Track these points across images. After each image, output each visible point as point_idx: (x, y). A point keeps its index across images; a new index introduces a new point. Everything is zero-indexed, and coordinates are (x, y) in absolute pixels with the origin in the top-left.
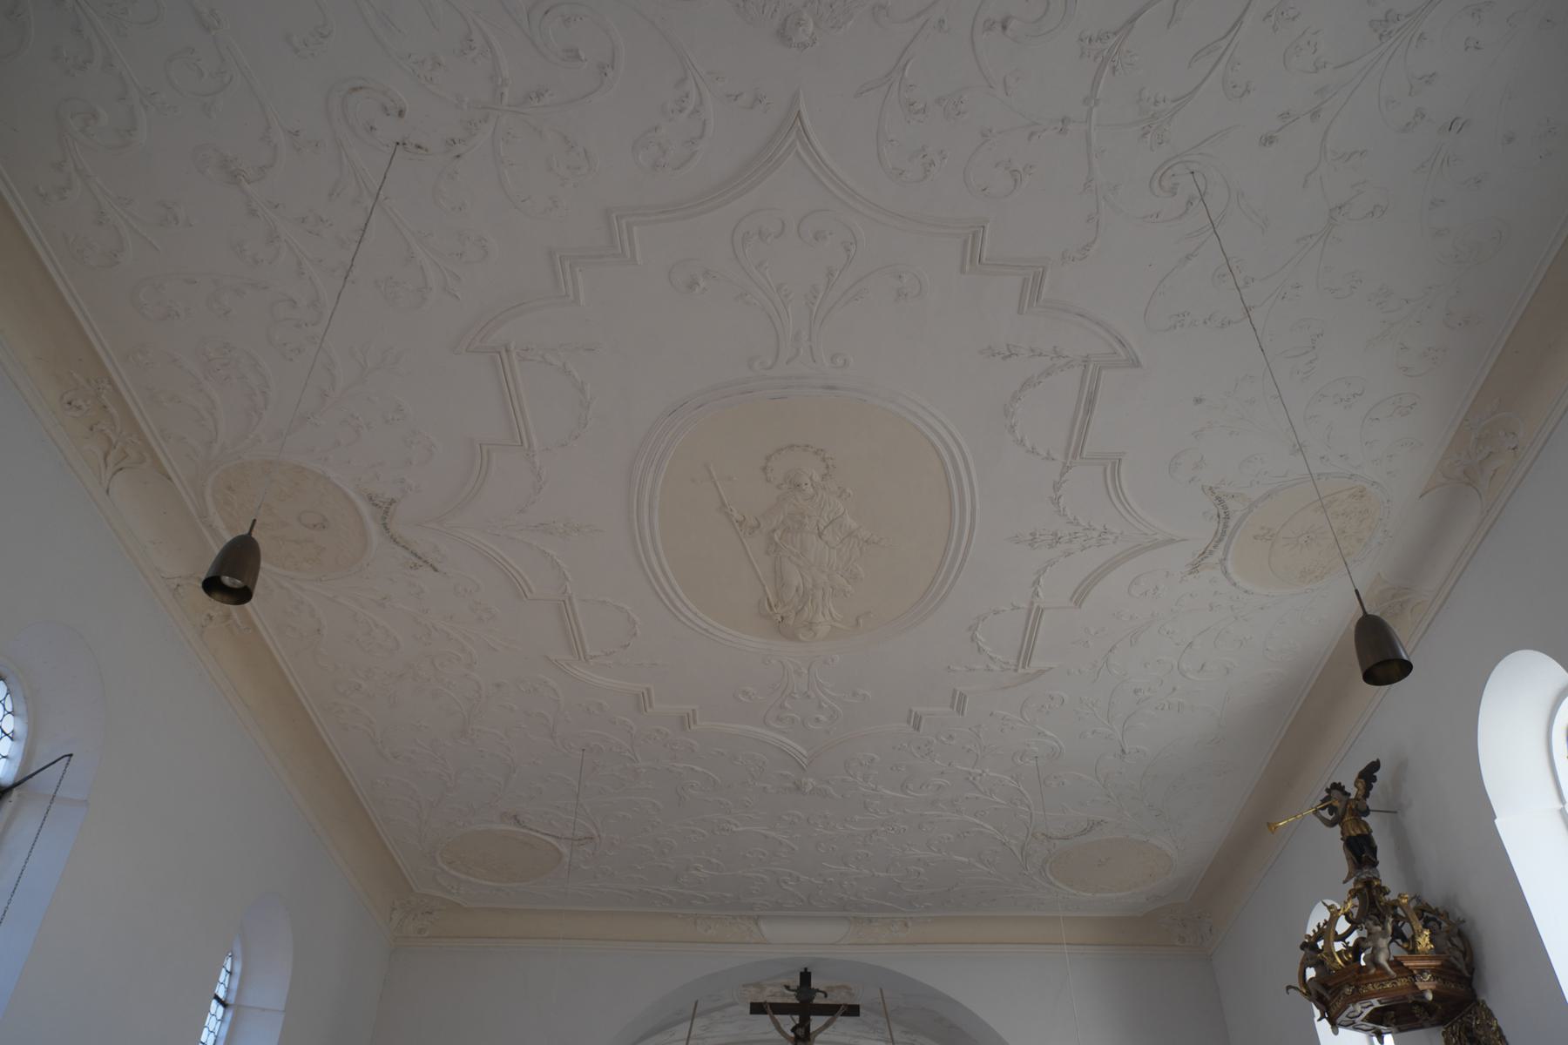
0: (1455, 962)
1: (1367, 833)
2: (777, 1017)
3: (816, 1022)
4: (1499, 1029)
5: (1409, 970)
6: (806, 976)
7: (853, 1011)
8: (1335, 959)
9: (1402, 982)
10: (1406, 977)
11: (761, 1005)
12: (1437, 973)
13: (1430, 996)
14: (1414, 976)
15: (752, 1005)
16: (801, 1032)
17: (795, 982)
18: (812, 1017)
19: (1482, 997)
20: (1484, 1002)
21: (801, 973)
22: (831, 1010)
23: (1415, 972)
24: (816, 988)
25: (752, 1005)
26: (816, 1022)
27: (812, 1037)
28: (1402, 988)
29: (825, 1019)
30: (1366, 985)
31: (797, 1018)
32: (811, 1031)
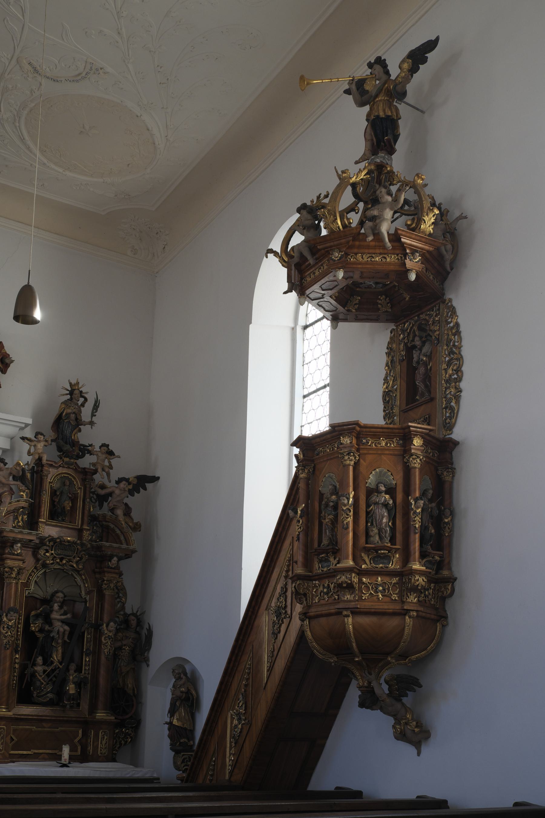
0: (445, 253)
1: (395, 118)
4: (457, 325)
5: (403, 247)
8: (336, 219)
9: (391, 259)
10: (398, 255)
12: (427, 258)
13: (413, 277)
14: (405, 255)
19: (449, 295)
20: (450, 300)
23: (408, 251)
28: (390, 264)
30: (356, 254)
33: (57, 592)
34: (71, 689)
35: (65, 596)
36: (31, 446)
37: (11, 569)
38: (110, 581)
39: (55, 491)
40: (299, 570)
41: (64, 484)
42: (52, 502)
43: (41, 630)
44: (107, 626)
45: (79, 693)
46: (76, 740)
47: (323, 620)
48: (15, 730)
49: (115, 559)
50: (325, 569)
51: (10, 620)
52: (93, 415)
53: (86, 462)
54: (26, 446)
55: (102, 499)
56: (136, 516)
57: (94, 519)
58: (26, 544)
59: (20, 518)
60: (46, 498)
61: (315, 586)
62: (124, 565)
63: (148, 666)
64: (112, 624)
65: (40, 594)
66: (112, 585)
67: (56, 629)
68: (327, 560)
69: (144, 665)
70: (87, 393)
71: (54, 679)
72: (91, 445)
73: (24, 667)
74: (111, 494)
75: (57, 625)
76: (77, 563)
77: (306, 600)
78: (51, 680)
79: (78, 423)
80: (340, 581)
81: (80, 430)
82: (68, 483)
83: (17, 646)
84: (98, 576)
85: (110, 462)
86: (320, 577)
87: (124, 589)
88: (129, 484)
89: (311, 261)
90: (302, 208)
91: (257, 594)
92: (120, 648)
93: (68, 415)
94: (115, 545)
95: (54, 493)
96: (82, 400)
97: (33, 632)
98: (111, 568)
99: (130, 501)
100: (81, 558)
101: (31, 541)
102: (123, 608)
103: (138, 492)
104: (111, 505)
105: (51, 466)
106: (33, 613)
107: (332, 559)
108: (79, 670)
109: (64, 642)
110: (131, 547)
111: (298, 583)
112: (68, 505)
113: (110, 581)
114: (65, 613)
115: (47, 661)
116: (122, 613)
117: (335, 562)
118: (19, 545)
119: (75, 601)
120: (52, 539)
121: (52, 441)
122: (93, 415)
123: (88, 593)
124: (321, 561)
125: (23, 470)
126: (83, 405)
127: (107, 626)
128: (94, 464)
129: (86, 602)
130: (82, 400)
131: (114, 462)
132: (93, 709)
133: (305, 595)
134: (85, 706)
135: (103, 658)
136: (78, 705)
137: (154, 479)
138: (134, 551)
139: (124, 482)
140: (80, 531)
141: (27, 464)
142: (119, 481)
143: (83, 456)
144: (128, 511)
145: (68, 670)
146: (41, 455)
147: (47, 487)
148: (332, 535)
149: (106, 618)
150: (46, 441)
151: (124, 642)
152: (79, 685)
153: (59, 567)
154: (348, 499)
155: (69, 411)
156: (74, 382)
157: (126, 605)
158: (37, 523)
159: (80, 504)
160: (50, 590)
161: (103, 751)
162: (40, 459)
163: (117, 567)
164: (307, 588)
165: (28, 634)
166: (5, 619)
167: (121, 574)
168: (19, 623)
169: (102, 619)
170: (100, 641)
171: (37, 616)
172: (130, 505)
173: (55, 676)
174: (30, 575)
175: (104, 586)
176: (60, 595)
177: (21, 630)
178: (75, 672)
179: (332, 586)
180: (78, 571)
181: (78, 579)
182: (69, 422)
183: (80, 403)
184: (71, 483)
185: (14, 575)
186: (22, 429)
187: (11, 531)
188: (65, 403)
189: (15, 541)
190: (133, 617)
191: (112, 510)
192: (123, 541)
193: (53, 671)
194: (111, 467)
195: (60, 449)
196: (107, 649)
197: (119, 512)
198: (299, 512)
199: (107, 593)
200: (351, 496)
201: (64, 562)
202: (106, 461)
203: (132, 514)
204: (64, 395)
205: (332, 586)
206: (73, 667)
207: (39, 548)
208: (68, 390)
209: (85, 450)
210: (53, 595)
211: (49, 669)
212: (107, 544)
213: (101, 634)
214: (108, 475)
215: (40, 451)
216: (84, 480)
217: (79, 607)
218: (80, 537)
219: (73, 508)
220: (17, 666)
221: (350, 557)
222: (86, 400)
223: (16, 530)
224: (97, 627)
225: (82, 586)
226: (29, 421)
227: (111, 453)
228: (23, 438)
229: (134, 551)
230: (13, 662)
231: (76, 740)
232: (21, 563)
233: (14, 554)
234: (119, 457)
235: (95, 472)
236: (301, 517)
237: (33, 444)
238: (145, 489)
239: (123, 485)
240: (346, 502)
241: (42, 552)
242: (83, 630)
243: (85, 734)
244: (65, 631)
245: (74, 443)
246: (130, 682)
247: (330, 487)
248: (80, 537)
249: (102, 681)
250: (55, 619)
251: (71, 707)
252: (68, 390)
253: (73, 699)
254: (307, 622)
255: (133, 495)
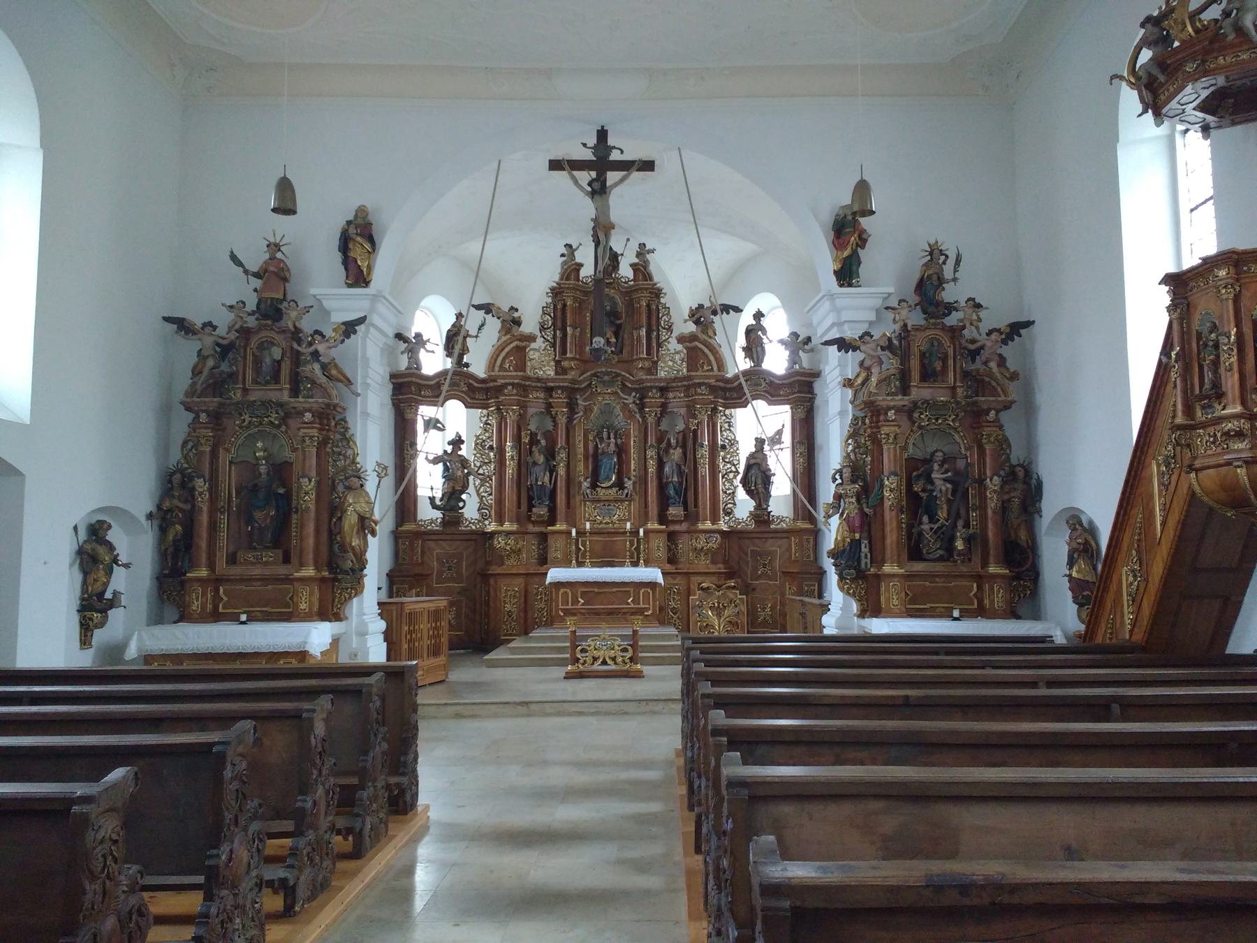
2: (575, 173)
3: (612, 177)
6: (602, 134)
7: (648, 166)
11: (559, 161)
15: (551, 162)
16: (596, 186)
17: (592, 141)
18: (608, 173)
21: (598, 131)
22: (626, 166)
24: (612, 145)
25: (551, 162)
26: (612, 177)
27: (608, 190)
29: (621, 174)
31: (594, 174)
32: (609, 183)
33: (936, 451)
34: (959, 545)
35: (945, 454)
36: (895, 314)
37: (888, 435)
38: (989, 436)
39: (925, 353)
40: (1180, 420)
41: (932, 345)
42: (923, 366)
43: (923, 490)
44: (991, 480)
45: (970, 549)
46: (972, 594)
47: (1211, 471)
48: (909, 586)
49: (993, 412)
50: (1209, 416)
51: (892, 484)
52: (955, 271)
53: (953, 320)
54: (890, 315)
55: (974, 354)
56: (1012, 365)
57: (966, 375)
58: (899, 410)
59: (892, 385)
60: (915, 364)
61: (1200, 436)
62: (1005, 417)
63: (1041, 516)
64: (995, 478)
65: (919, 455)
66: (992, 439)
67: (938, 488)
68: (1210, 406)
69: (1036, 516)
70: (947, 250)
71: (942, 536)
72: (956, 302)
73: (910, 527)
74: (982, 347)
75: (938, 483)
76: (953, 421)
77: (1191, 451)
78: (939, 537)
79: (941, 281)
80: (1226, 429)
81: (944, 289)
82: (936, 343)
83: (902, 507)
84: (976, 431)
85: (978, 316)
86: (1204, 426)
87: (1006, 440)
88: (1001, 333)
89: (1162, 78)
90: (1148, 20)
91: (1141, 443)
92: (1009, 500)
93: (929, 277)
94: (991, 399)
95: (923, 355)
96: (943, 258)
97: (916, 493)
98: (990, 422)
99: (1006, 351)
100: (957, 416)
101: (904, 406)
102: (1008, 459)
103: (1013, 340)
104: (984, 358)
105: (917, 329)
106: (915, 474)
107: (1216, 405)
108: (967, 525)
109: (949, 501)
110: (1010, 399)
111: (1178, 433)
112: (938, 366)
113: (989, 436)
114: (946, 472)
115: (932, 519)
116: (1008, 464)
117: (1220, 407)
118: (893, 411)
119: (955, 458)
120: (926, 401)
121: (916, 305)
122: (955, 271)
123: (969, 448)
124: (1203, 408)
125: (890, 339)
126: (944, 263)
127: (991, 480)
128: (961, 321)
129: (967, 458)
130: (943, 258)
131: (983, 314)
132: (985, 564)
133: (1188, 446)
134: (977, 559)
135: (990, 512)
136: (970, 560)
137: (1028, 324)
138: (1013, 402)
139: (996, 333)
140: (953, 388)
141: (894, 332)
142: (990, 333)
143: (949, 314)
144: (1002, 361)
145: (955, 526)
146: (906, 321)
147: (915, 351)
148: (1216, 377)
149: (989, 473)
150: (910, 306)
151: (1012, 494)
152: (969, 540)
153: (936, 427)
154: (1229, 337)
155: (931, 272)
156: (932, 242)
157: (1011, 456)
158: (909, 387)
159: (951, 362)
160: (930, 450)
161: (1000, 604)
162: (905, 325)
163: (997, 420)
164: (1190, 438)
165: (912, 497)
166: (887, 483)
167: (1001, 427)
168: (901, 485)
169: (985, 473)
170: (986, 497)
171: (919, 476)
172: (1004, 355)
173: (943, 533)
174: (907, 438)
175: (984, 441)
176: (940, 454)
177: (904, 492)
178: (964, 527)
179: (1219, 435)
180: (955, 429)
181: (957, 437)
182: (932, 283)
183: (941, 261)
184: (940, 343)
185: (891, 441)
186: (885, 299)
187: (884, 400)
188: (926, 265)
189: (889, 408)
190: (1019, 468)
191: (985, 363)
192: (1001, 393)
193: (939, 528)
194: (980, 320)
195: (925, 312)
196: (993, 503)
197: (993, 365)
198: (1173, 356)
199: (988, 447)
200: (1233, 333)
201: (940, 421)
202: (974, 315)
203: (1008, 364)
204: (924, 257)
205: (1219, 435)
206: (960, 523)
207: (913, 412)
208: (926, 251)
209: (950, 308)
210: (933, 454)
211: (936, 527)
212: (983, 399)
213: (986, 488)
214: (977, 328)
215: (904, 318)
216: (953, 339)
217: (961, 464)
218: (954, 394)
219: (945, 367)
220: (904, 526)
221: (1238, 402)
222: (947, 257)
223: (889, 398)
224: (981, 482)
225: (961, 442)
226: (891, 290)
227: (979, 306)
228: (887, 308)
229: (1013, 402)
230: (899, 523)
231: (972, 594)
232: (896, 428)
233: (889, 421)
234: (987, 308)
235: (964, 327)
236: (1176, 361)
237: (897, 312)
238: (1020, 336)
239: (994, 336)
240: (1226, 340)
241: (916, 415)
242: (966, 486)
243: (979, 587)
244: (947, 489)
245: (939, 304)
246: (1023, 535)
247: (1208, 325)
248: (954, 394)
249: (990, 534)
250: (937, 478)
251: (963, 562)
252: (926, 251)
253: (964, 555)
254: (1193, 475)
255: (1007, 345)
